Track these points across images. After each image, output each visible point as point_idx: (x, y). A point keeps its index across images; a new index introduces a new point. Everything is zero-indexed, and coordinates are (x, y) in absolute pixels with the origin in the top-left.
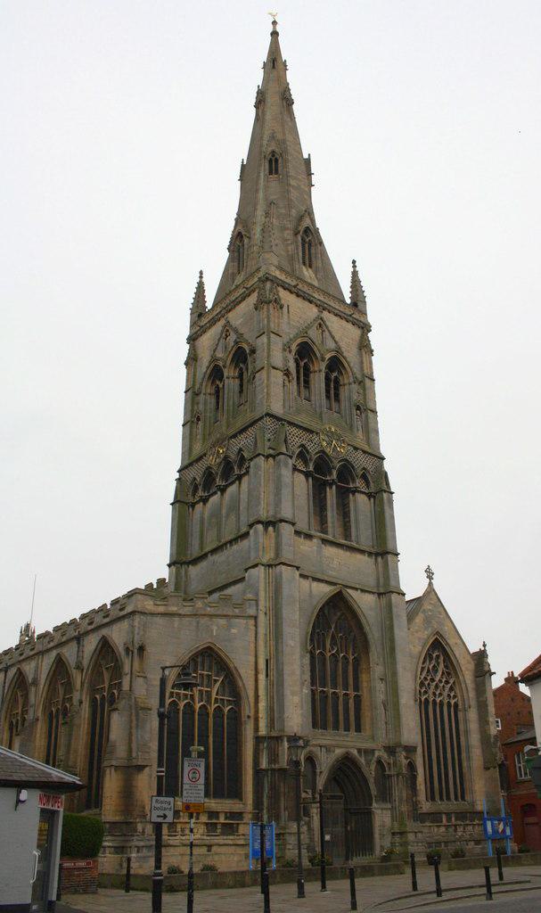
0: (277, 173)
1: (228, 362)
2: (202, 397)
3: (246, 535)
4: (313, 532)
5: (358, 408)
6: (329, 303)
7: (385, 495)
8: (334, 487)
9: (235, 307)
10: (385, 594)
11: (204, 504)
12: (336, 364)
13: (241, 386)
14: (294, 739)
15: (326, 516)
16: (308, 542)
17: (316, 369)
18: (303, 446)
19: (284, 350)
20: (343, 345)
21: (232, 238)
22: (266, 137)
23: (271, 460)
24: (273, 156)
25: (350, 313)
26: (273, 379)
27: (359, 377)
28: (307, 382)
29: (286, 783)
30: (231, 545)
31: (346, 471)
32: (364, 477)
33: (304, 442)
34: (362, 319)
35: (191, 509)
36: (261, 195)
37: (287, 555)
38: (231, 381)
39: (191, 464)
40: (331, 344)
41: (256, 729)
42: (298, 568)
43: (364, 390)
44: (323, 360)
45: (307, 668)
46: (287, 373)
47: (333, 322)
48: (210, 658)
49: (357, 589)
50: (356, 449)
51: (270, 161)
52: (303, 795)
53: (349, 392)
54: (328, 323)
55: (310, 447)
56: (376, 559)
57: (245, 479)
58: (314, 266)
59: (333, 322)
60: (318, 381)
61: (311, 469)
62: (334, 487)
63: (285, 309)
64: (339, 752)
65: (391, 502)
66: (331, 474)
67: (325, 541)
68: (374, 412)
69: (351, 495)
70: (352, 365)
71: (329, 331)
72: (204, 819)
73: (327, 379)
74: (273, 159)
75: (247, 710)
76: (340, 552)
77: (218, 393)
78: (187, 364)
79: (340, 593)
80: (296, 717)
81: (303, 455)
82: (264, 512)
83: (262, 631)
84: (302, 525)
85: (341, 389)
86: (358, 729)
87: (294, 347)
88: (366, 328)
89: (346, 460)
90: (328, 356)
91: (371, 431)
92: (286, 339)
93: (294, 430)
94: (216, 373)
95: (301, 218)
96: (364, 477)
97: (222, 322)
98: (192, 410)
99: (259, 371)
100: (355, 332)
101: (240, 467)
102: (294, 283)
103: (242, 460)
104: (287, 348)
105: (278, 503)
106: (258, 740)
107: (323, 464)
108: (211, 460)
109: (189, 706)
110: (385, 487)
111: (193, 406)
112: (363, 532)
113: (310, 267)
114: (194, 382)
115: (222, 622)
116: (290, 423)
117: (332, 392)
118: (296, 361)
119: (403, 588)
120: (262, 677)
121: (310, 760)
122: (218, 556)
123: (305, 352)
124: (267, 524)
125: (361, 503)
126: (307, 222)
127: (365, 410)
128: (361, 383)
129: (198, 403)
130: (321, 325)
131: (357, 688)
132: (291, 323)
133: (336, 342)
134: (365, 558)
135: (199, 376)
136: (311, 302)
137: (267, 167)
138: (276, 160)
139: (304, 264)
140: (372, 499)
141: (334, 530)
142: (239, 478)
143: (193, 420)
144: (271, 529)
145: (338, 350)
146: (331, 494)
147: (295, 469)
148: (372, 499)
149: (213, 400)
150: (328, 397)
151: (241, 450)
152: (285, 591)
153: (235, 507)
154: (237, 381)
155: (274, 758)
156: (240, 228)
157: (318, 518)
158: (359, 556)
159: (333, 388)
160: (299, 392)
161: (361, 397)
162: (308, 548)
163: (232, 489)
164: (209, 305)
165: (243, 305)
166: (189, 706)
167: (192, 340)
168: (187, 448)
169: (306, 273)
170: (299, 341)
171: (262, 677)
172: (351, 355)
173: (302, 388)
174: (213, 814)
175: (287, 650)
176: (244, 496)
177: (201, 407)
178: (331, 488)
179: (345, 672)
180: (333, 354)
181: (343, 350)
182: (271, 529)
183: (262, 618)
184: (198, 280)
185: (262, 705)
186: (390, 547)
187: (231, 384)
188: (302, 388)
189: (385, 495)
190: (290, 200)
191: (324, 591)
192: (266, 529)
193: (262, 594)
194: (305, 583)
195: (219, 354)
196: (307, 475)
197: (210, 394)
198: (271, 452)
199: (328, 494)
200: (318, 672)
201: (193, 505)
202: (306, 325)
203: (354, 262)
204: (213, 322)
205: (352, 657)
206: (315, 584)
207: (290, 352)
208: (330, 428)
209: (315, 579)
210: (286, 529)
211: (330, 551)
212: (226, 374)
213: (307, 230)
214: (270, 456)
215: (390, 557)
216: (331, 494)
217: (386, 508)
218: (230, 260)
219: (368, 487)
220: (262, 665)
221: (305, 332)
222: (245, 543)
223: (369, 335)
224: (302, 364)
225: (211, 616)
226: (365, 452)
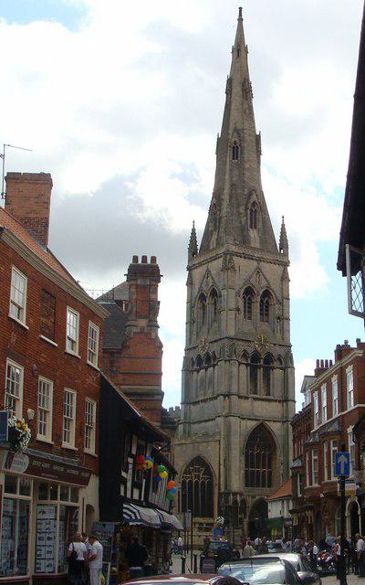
3: (216, 398)
5: (279, 318)
12: (267, 294)
13: (215, 309)
14: (235, 494)
20: (272, 281)
22: (231, 131)
26: (229, 316)
27: (280, 298)
28: (250, 308)
29: (233, 512)
31: (269, 358)
32: (279, 359)
36: (227, 177)
37: (234, 411)
40: (264, 283)
41: (219, 489)
45: (243, 461)
47: (266, 267)
48: (199, 462)
50: (275, 345)
52: (239, 516)
53: (275, 310)
54: (263, 270)
57: (216, 367)
59: (266, 267)
60: (256, 308)
64: (257, 498)
67: (255, 399)
68: (288, 319)
72: (197, 525)
73: (261, 301)
75: (216, 482)
76: (264, 403)
77: (204, 307)
79: (261, 424)
80: (237, 483)
81: (245, 355)
82: (223, 390)
83: (222, 446)
84: (243, 392)
91: (285, 332)
93: (241, 343)
94: (202, 297)
95: (250, 195)
97: (205, 267)
100: (279, 269)
101: (215, 359)
103: (215, 357)
104: (237, 294)
105: (230, 386)
106: (220, 494)
108: (202, 353)
109: (191, 482)
112: (277, 391)
113: (255, 228)
115: (204, 444)
116: (238, 340)
120: (222, 467)
121: (244, 501)
124: (225, 396)
125: (277, 374)
126: (254, 198)
127: (283, 319)
128: (281, 304)
130: (259, 271)
131: (270, 467)
134: (277, 403)
139: (251, 227)
141: (262, 394)
142: (214, 366)
143: (191, 322)
146: (260, 372)
147: (240, 363)
150: (261, 314)
152: (233, 428)
153: (211, 382)
155: (227, 502)
158: (274, 403)
159: (265, 308)
162: (246, 404)
163: (211, 369)
164: (199, 247)
166: (191, 482)
167: (189, 269)
169: (252, 236)
171: (222, 467)
172: (275, 286)
173: (247, 314)
174: (201, 524)
175: (233, 455)
176: (216, 375)
179: (264, 461)
183: (222, 440)
185: (222, 479)
186: (290, 398)
187: (210, 308)
188: (247, 314)
190: (244, 182)
191: (253, 424)
193: (222, 429)
194: (243, 422)
195: (204, 288)
196: (247, 365)
200: (249, 460)
201: (192, 372)
204: (200, 264)
210: (234, 398)
213: (254, 203)
215: (289, 403)
216: (260, 372)
220: (222, 462)
225: (199, 443)
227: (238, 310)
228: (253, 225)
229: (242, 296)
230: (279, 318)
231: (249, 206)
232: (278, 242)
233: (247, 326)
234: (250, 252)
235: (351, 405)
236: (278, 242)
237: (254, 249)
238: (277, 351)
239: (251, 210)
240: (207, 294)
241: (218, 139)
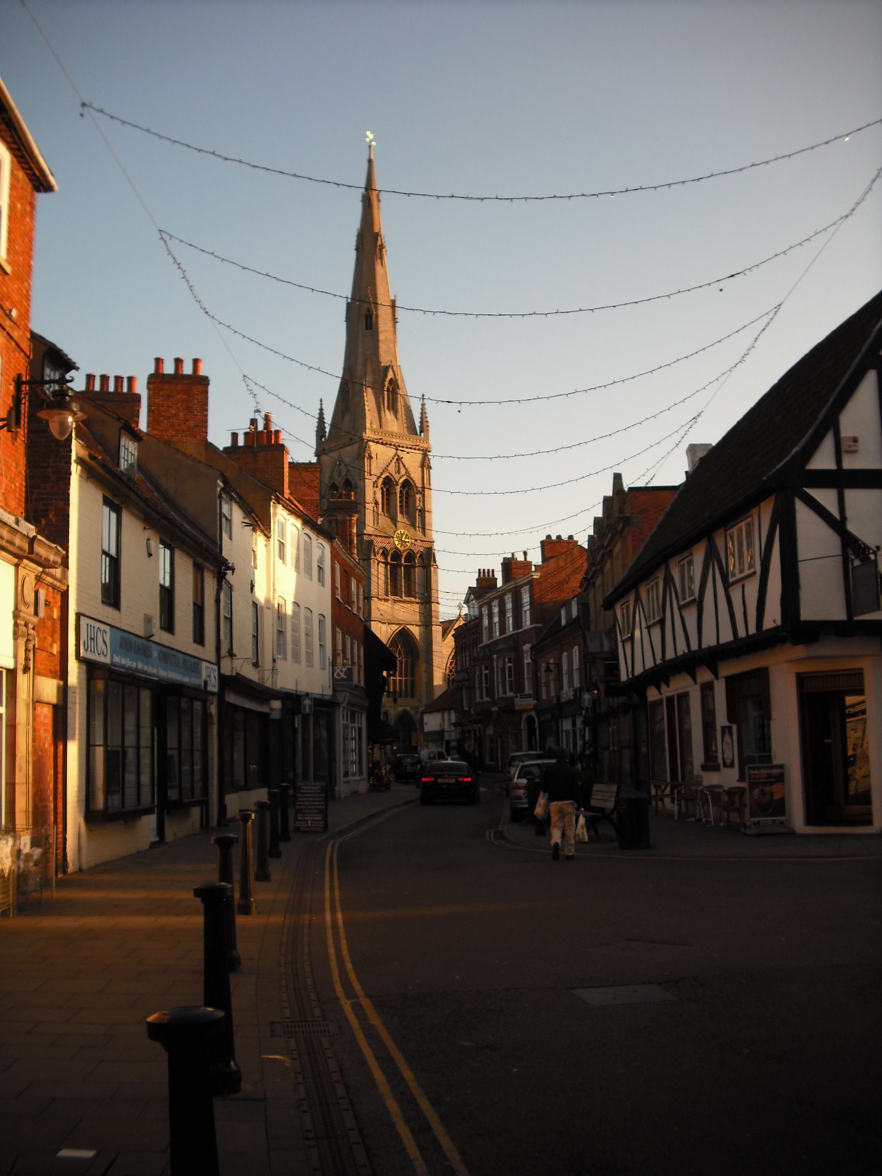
12: (408, 484)
16: (386, 603)
31: (411, 556)
36: (360, 350)
43: (424, 496)
46: (376, 503)
64: (400, 708)
65: (436, 572)
67: (395, 601)
81: (385, 553)
86: (413, 696)
87: (380, 481)
88: (425, 453)
90: (401, 481)
93: (379, 539)
104: (375, 484)
107: (397, 555)
113: (393, 409)
116: (376, 536)
123: (388, 483)
126: (390, 375)
128: (423, 493)
130: (399, 460)
131: (412, 675)
137: (364, 321)
139: (388, 409)
160: (383, 511)
164: (327, 430)
170: (383, 476)
172: (416, 476)
180: (405, 478)
195: (336, 477)
196: (386, 564)
205: (409, 661)
211: (397, 606)
213: (391, 380)
221: (385, 469)
227: (376, 503)
228: (393, 407)
229: (380, 487)
230: (420, 511)
232: (418, 425)
233: (384, 521)
234: (386, 439)
235: (527, 623)
236: (418, 425)
237: (392, 434)
238: (419, 548)
239: (388, 391)
240: (339, 482)
241: (348, 304)
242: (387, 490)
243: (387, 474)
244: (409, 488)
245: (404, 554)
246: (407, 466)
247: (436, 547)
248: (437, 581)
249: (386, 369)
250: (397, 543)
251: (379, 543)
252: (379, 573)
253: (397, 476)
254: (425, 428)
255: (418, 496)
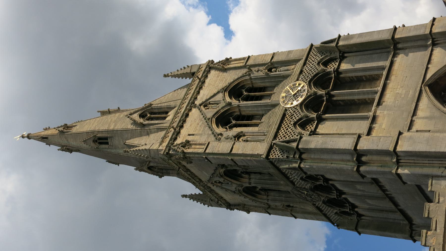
0: (106, 138)
1: (238, 183)
2: (272, 204)
4: (371, 114)
5: (270, 70)
6: (189, 98)
7: (341, 43)
8: (332, 93)
9: (196, 176)
10: (433, 39)
11: (356, 207)
12: (235, 91)
15: (359, 100)
16: (379, 120)
17: (237, 110)
18: (295, 124)
19: (220, 140)
21: (154, 174)
23: (304, 156)
24: (96, 141)
25: (198, 80)
26: (240, 152)
27: (244, 71)
30: (387, 190)
31: (319, 80)
33: (292, 123)
34: (203, 69)
35: (363, 218)
38: (252, 181)
39: (325, 215)
42: (400, 133)
44: (230, 104)
46: (238, 137)
49: (427, 68)
50: (301, 72)
51: (100, 143)
54: (204, 100)
55: (296, 117)
56: (400, 49)
58: (166, 110)
61: (314, 115)
62: (332, 93)
63: (190, 138)
66: (321, 96)
69: (342, 76)
70: (236, 77)
71: (210, 98)
74: (98, 141)
76: (391, 85)
78: (248, 212)
82: (351, 166)
84: (363, 126)
85: (255, 86)
87: (220, 130)
89: (310, 82)
90: (228, 99)
92: (212, 138)
94: (250, 191)
96: (326, 64)
98: (282, 210)
99: (235, 162)
102: (172, 130)
104: (218, 137)
107: (311, 103)
110: (334, 44)
111: (279, 210)
114: (260, 207)
117: (257, 94)
118: (231, 128)
119: (427, 20)
122: (399, 201)
123: (224, 119)
124: (360, 163)
129: (276, 206)
130: (205, 104)
132: (200, 132)
133: (218, 92)
135: (254, 204)
136: (187, 115)
137: (103, 146)
138: (100, 139)
139: (165, 118)
140: (346, 55)
142: (327, 180)
144: (364, 159)
145: (224, 90)
146: (340, 94)
148: (346, 55)
149: (272, 194)
151: (302, 179)
154: (252, 176)
156: (145, 168)
157: (362, 106)
160: (256, 125)
161: (261, 68)
165: (193, 170)
168: (312, 216)
170: (214, 126)
173: (254, 121)
177: (278, 204)
178: (333, 96)
180: (227, 94)
181: (224, 85)
182: (364, 159)
184: (188, 199)
186: (387, 36)
187: (254, 181)
189: (341, 43)
192: (364, 163)
194: (418, 124)
195: (233, 188)
196: (320, 120)
197: (268, 196)
198: (297, 156)
199: (339, 98)
202: (203, 119)
203: (165, 76)
206: (420, 113)
207: (221, 134)
208: (283, 97)
209: (414, 114)
211: (389, 97)
212: (248, 185)
213: (142, 116)
214: (300, 157)
216: (340, 94)
217: (352, 42)
218: (168, 174)
219: (336, 59)
221: (208, 120)
222: (380, 180)
223: (216, 61)
224: (234, 122)
226: (305, 64)
231: (141, 120)
242: (239, 118)
243: (214, 120)
244: (243, 87)
245: (314, 89)
246: (215, 91)
247: (317, 43)
248: (361, 35)
249: (135, 123)
250: (295, 103)
251: (290, 132)
252: (336, 134)
253: (223, 104)
254: (188, 70)
255: (255, 74)
